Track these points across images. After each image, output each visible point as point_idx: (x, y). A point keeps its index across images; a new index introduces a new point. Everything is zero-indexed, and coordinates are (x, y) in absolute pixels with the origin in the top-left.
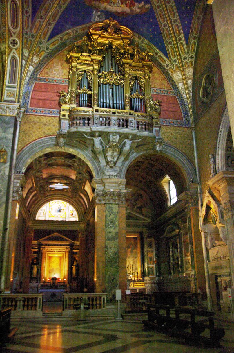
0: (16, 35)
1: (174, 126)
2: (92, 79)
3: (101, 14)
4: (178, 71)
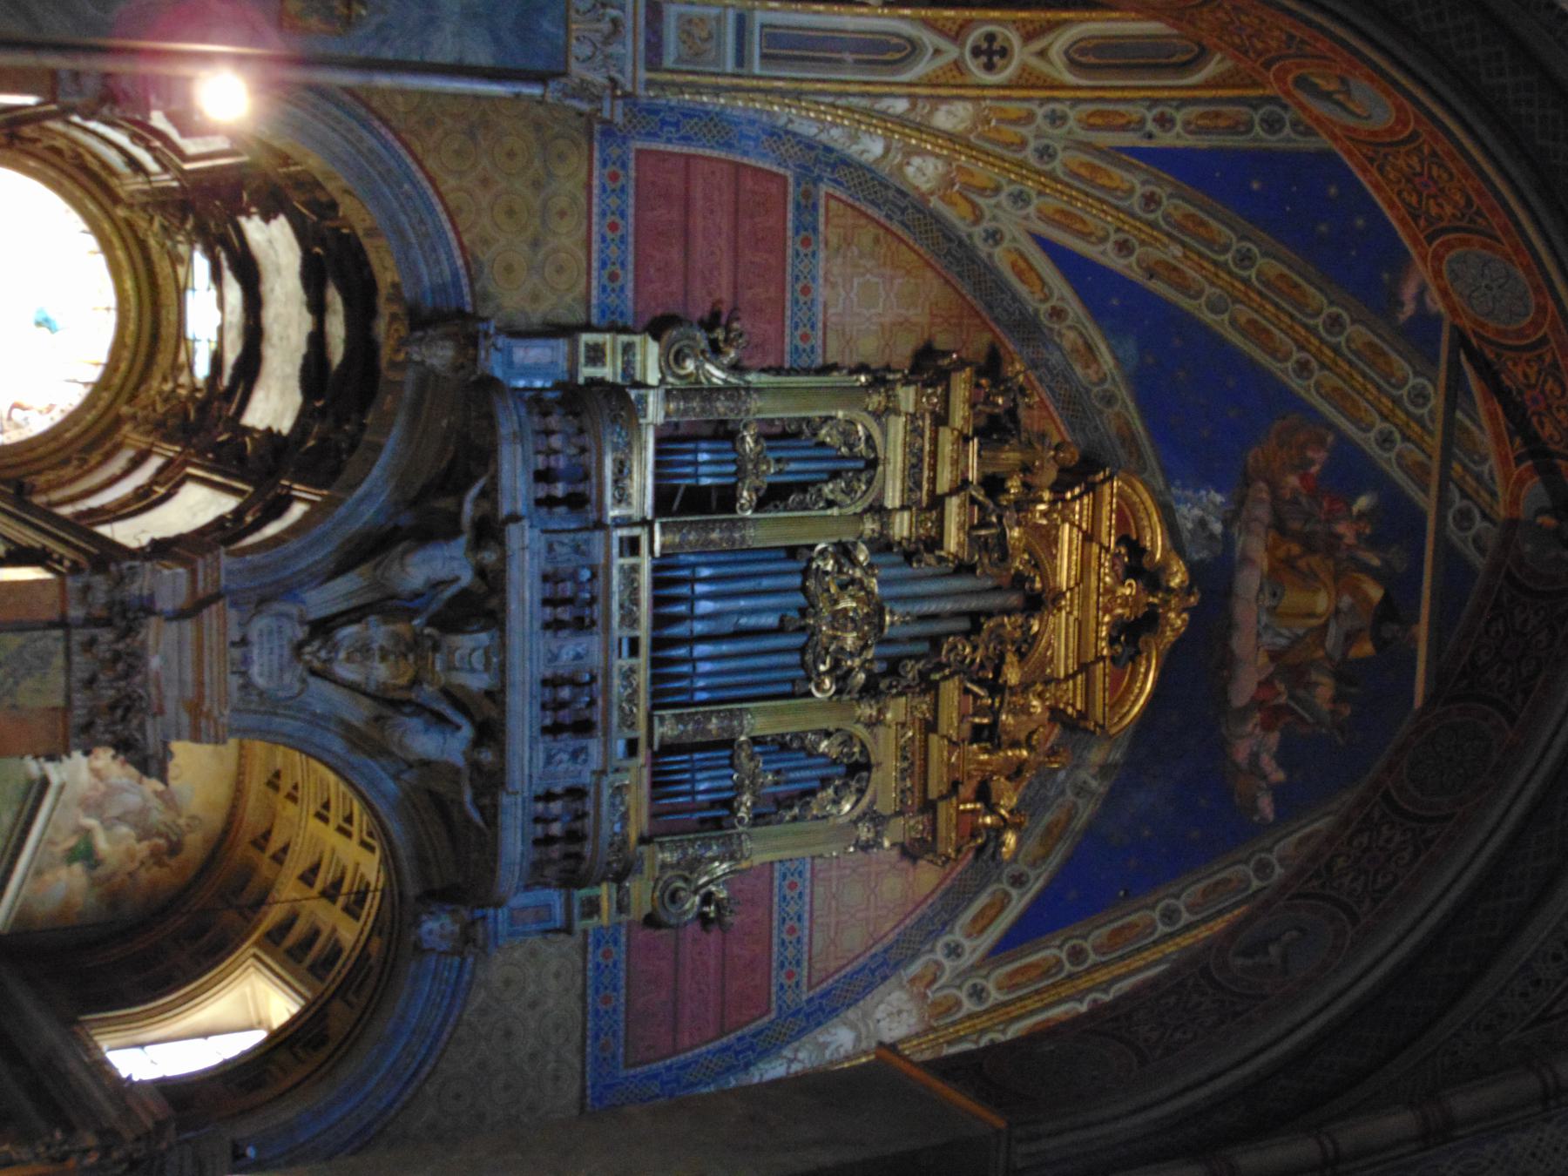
0: (1034, 62)
1: (584, 1014)
2: (830, 504)
3: (1212, 536)
4: (922, 1019)
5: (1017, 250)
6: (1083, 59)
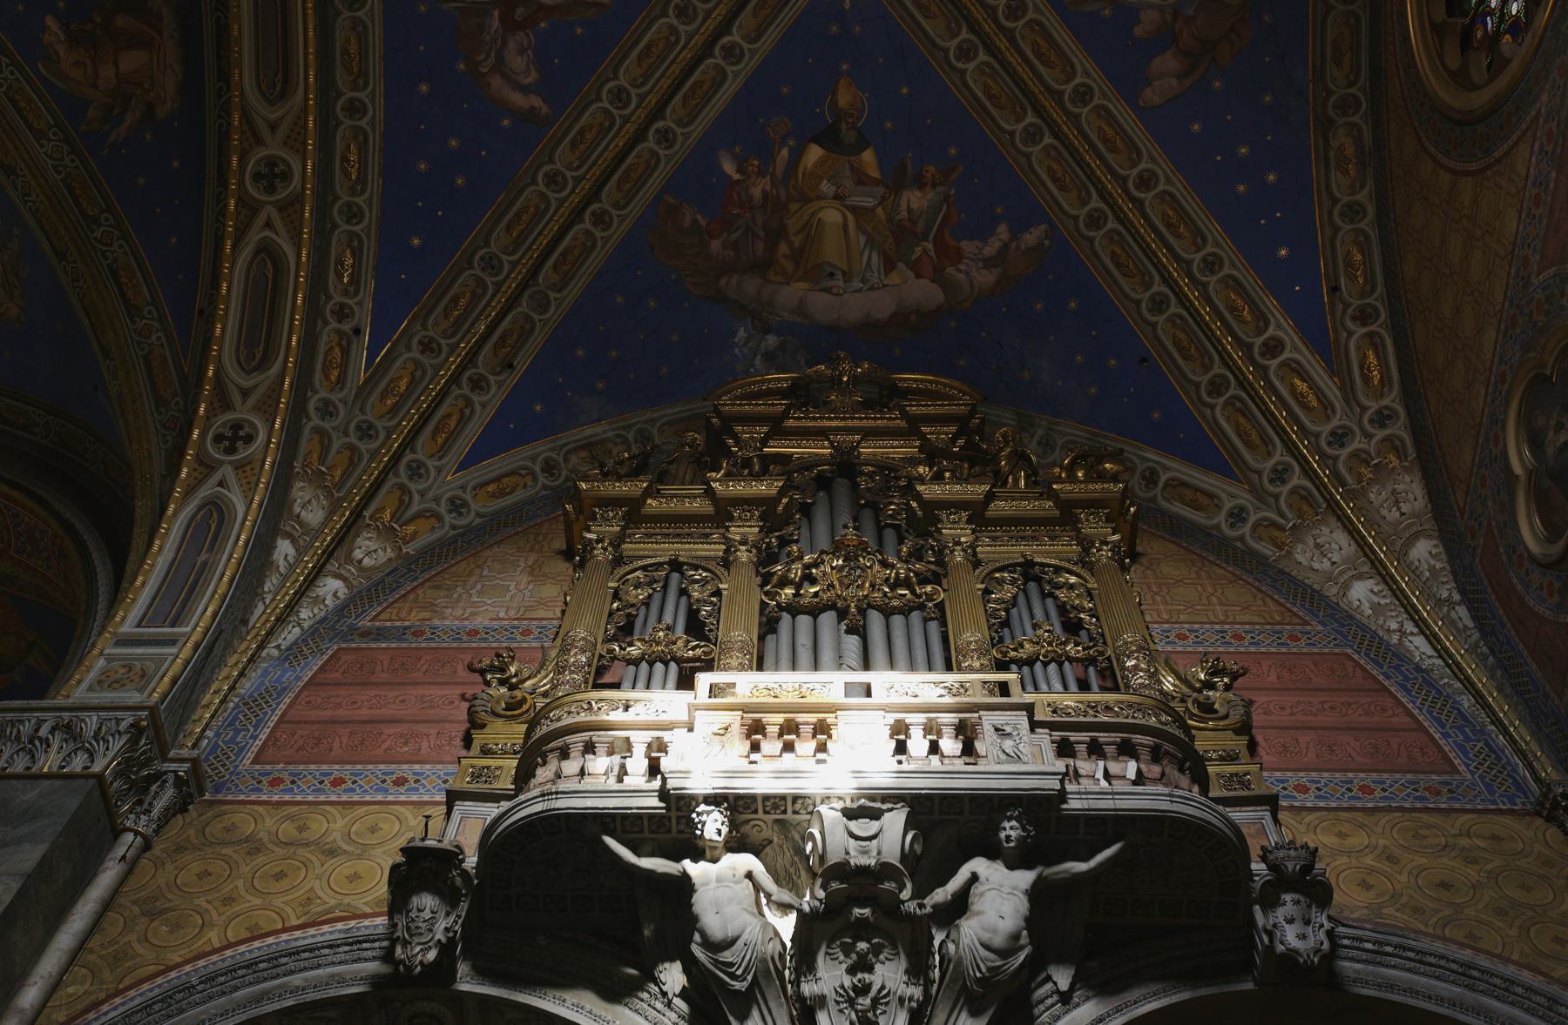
1: (1390, 809)
5: (474, 489)
6: (258, 357)
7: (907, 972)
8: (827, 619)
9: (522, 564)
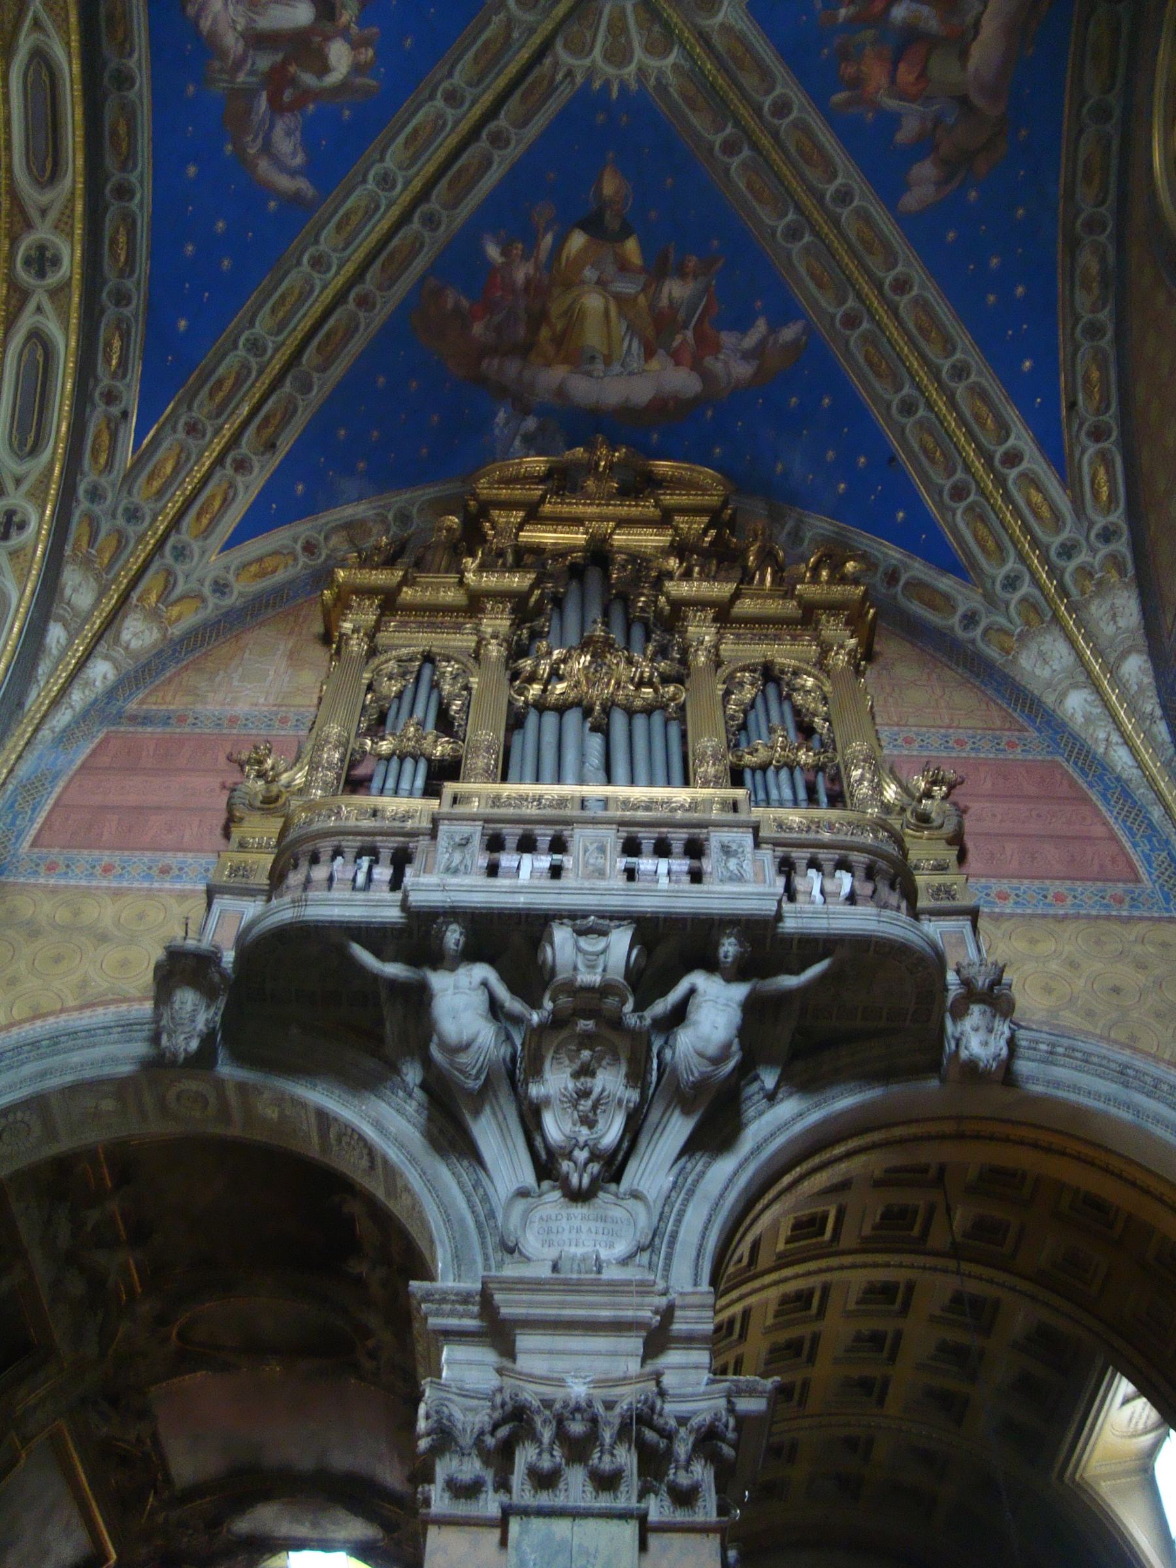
1: (1077, 917)
3: (541, 428)
7: (627, 1076)
8: (573, 718)
9: (282, 647)
